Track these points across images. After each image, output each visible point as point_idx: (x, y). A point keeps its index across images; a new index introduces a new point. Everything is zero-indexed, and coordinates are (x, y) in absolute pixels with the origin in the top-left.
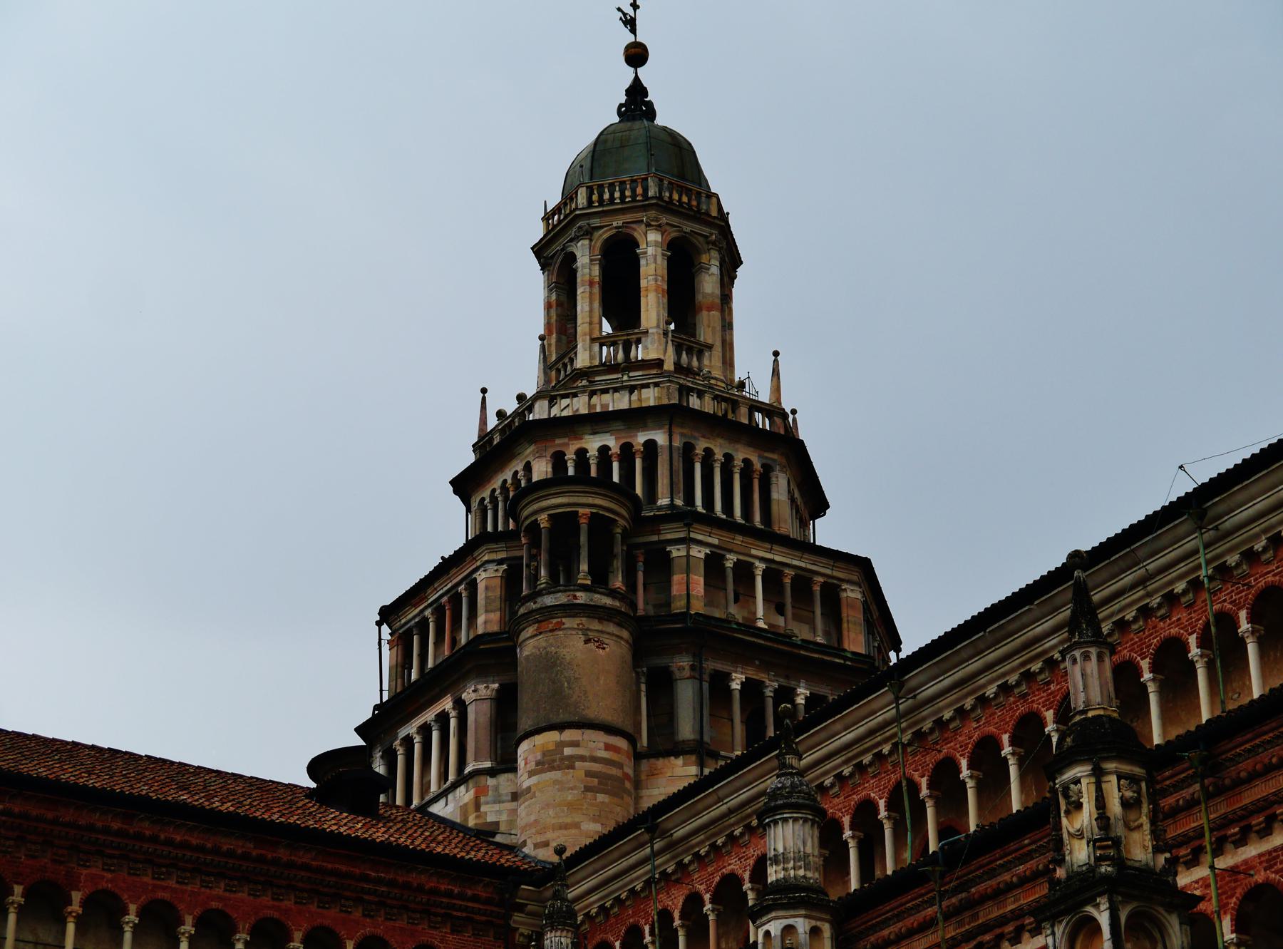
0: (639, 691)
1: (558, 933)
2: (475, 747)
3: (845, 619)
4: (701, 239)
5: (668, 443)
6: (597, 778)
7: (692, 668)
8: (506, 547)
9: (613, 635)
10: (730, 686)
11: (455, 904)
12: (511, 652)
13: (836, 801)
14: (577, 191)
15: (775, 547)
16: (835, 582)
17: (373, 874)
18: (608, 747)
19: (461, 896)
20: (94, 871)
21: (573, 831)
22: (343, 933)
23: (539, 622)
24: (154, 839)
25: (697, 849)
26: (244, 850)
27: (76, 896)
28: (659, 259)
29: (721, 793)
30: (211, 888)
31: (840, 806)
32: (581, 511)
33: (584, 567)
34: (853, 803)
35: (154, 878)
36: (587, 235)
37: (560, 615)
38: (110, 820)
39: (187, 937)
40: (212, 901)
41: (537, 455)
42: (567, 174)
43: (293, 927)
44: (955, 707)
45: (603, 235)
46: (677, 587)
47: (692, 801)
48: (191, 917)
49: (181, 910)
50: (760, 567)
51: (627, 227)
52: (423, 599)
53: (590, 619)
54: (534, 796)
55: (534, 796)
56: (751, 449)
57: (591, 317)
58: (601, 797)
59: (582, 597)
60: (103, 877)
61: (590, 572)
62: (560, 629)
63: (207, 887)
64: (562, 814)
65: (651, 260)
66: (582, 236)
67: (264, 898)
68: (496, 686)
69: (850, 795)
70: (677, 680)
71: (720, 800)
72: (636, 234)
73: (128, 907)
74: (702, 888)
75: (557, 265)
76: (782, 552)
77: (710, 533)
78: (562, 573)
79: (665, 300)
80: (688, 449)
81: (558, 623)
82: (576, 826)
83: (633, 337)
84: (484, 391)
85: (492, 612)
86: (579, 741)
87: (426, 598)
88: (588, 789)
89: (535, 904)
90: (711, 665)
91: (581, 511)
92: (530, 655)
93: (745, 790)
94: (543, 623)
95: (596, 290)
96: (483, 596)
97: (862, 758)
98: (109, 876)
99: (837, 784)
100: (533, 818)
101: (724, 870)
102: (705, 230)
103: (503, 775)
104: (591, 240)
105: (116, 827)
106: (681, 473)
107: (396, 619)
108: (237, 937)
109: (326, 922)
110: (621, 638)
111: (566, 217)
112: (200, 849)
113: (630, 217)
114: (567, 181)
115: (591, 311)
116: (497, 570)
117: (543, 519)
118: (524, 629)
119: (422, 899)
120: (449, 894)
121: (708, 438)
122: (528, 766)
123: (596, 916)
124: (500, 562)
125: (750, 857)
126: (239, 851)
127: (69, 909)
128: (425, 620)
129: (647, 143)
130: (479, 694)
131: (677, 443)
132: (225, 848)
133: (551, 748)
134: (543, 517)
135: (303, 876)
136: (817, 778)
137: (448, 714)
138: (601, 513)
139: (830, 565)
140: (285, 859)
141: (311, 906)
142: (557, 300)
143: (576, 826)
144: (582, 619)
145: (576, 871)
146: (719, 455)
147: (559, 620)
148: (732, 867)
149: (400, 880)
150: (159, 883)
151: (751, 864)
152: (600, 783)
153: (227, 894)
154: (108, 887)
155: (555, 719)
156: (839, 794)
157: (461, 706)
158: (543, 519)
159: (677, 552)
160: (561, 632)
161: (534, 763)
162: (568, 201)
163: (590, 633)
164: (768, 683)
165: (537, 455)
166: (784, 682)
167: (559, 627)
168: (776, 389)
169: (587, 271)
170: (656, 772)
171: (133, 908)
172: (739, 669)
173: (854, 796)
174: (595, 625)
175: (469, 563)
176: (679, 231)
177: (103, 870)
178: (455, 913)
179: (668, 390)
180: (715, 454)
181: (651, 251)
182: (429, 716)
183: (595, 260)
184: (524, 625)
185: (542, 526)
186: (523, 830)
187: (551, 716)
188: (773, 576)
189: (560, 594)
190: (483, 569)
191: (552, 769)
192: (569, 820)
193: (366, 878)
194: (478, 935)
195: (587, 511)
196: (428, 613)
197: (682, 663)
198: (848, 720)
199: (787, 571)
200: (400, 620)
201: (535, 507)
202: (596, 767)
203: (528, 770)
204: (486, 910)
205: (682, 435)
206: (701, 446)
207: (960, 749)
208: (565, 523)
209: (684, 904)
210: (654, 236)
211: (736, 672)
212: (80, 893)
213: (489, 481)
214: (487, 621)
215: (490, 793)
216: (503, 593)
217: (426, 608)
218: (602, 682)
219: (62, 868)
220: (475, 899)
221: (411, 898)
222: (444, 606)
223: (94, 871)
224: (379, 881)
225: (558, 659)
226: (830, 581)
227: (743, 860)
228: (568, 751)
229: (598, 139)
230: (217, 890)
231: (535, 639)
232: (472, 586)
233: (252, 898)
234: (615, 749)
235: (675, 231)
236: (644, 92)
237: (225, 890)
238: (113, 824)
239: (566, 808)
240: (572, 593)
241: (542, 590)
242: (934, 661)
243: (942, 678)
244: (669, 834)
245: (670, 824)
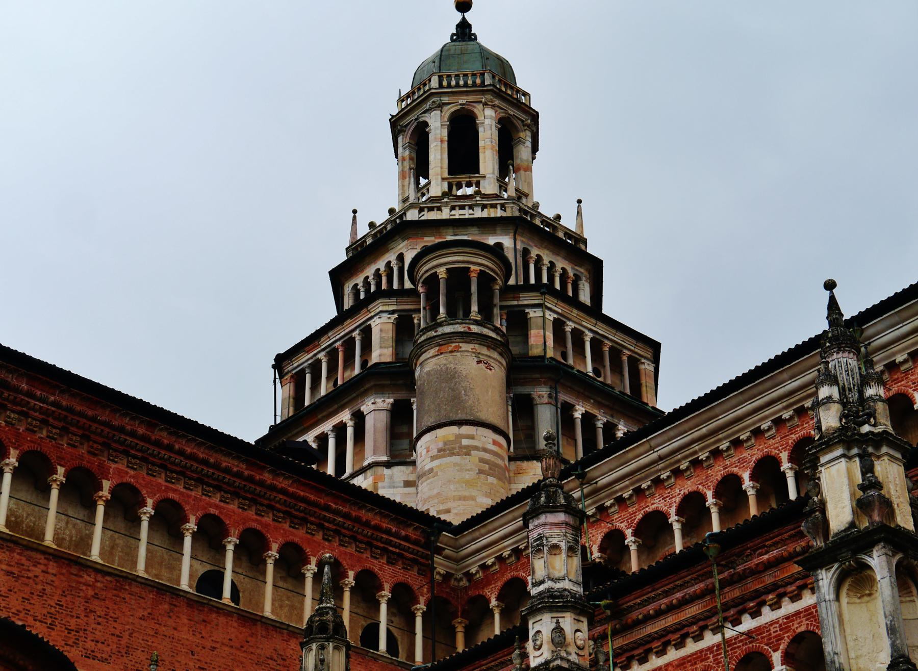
0: (508, 411)
1: (846, 354)
2: (374, 446)
3: (644, 384)
4: (520, 122)
5: (513, 246)
6: (488, 464)
7: (550, 396)
8: (397, 302)
9: (497, 360)
10: (573, 415)
11: (392, 541)
13: (771, 442)
14: (430, 79)
15: (599, 323)
16: (637, 356)
17: (334, 506)
18: (495, 443)
19: (396, 535)
20: (120, 466)
21: (471, 502)
22: (308, 550)
23: (440, 345)
24: (169, 448)
25: (620, 494)
26: (238, 469)
27: (106, 485)
28: (494, 128)
29: (653, 443)
30: (210, 497)
31: (776, 445)
32: (473, 267)
33: (475, 308)
34: (790, 442)
35: (166, 481)
36: (439, 107)
37: (459, 340)
38: (136, 426)
39: (191, 533)
40: (210, 507)
41: (410, 248)
42: (415, 74)
43: (271, 539)
44: (909, 351)
45: (452, 109)
47: (624, 451)
48: (195, 517)
49: (187, 510)
50: (588, 336)
51: (468, 105)
52: (317, 346)
53: (482, 346)
54: (436, 474)
55: (436, 474)
56: (567, 262)
57: (441, 164)
58: (491, 479)
59: (475, 329)
60: (127, 473)
61: (480, 312)
62: (458, 351)
63: (206, 495)
64: (461, 489)
65: (487, 128)
66: (435, 107)
67: (250, 512)
68: (391, 400)
69: (788, 436)
70: (537, 404)
71: (652, 448)
72: (476, 111)
73: (146, 500)
74: (623, 526)
75: (410, 132)
76: (603, 328)
77: (556, 304)
78: (458, 309)
79: (497, 158)
80: (526, 252)
81: (456, 346)
82: (473, 498)
83: (474, 179)
84: (355, 212)
85: (385, 348)
86: (474, 435)
87: (319, 345)
88: (481, 472)
89: (451, 549)
90: (563, 397)
91: (473, 267)
92: (431, 371)
93: (679, 438)
94: (443, 347)
95: (445, 145)
96: (378, 336)
97: (804, 403)
98: (132, 472)
99: (774, 427)
100: (435, 491)
101: (647, 509)
102: (522, 116)
103: (396, 467)
104: (441, 112)
105: (141, 432)
106: (522, 268)
107: (290, 363)
108: (229, 540)
109: (296, 540)
110: (502, 365)
111: (425, 92)
112: (205, 462)
113: (471, 98)
114: (416, 77)
115: (442, 159)
116: (389, 318)
117: (442, 273)
118: (425, 351)
119: (368, 532)
120: (388, 532)
121: (539, 248)
122: (429, 453)
123: (508, 558)
124: (393, 312)
125: (675, 496)
126: (235, 469)
127: (101, 493)
128: (319, 362)
129: (481, 53)
131: (520, 246)
132: (224, 464)
133: (451, 439)
134: (441, 270)
135: (281, 499)
136: (754, 423)
137: (345, 424)
138: (487, 271)
139: (634, 344)
140: (269, 482)
141: (285, 525)
142: (410, 155)
143: (473, 498)
144: (476, 345)
145: (494, 520)
146: (546, 260)
147: (457, 344)
148: (656, 505)
149: (354, 514)
150: (170, 485)
151: (677, 501)
152: (490, 469)
153: (222, 504)
154: (131, 482)
155: (454, 417)
156: (775, 436)
157: (359, 418)
158: (442, 273)
159: (533, 313)
160: (459, 354)
161: (436, 450)
162: (421, 86)
163: (481, 357)
164: (599, 417)
165: (410, 248)
166: (610, 419)
167: (457, 349)
168: (580, 225)
169: (439, 132)
170: (521, 472)
171: (150, 502)
172: (581, 403)
173: (793, 436)
174: (484, 351)
175: (363, 314)
176: (506, 113)
177: (128, 467)
178: (391, 548)
179: (512, 209)
180: (543, 260)
181: (487, 122)
182: (327, 427)
183: (445, 125)
184: (426, 348)
185: (440, 277)
186: (426, 501)
187: (451, 415)
188: (597, 344)
189: (458, 325)
190: (378, 316)
191: (453, 454)
192: (466, 494)
193: (327, 508)
194: (407, 569)
195: (477, 268)
196: (321, 356)
197: (541, 393)
198: (796, 370)
199: (606, 342)
200: (293, 365)
201: (435, 263)
202: (487, 456)
203: (430, 456)
204: (414, 549)
205: (522, 242)
206: (534, 252)
207: (912, 386)
208: (458, 276)
209: (603, 540)
210: (489, 112)
211: (579, 405)
212: (109, 482)
213: (362, 271)
214: (381, 353)
215: (386, 480)
216: (394, 335)
217: (319, 352)
218: (490, 393)
219: (95, 459)
221: (360, 530)
222: (338, 349)
223: (120, 466)
224: (337, 512)
225: (456, 373)
226: (634, 355)
227: (668, 499)
228: (465, 442)
229: (443, 48)
230: (214, 499)
231: (436, 358)
232: (367, 332)
233: (240, 510)
234: (500, 446)
235: (503, 113)
236: (470, 26)
237: (221, 501)
238: (139, 430)
239: (464, 485)
240: (467, 325)
241: (442, 322)
242: (896, 311)
243: (901, 325)
244: (594, 481)
245: (596, 473)
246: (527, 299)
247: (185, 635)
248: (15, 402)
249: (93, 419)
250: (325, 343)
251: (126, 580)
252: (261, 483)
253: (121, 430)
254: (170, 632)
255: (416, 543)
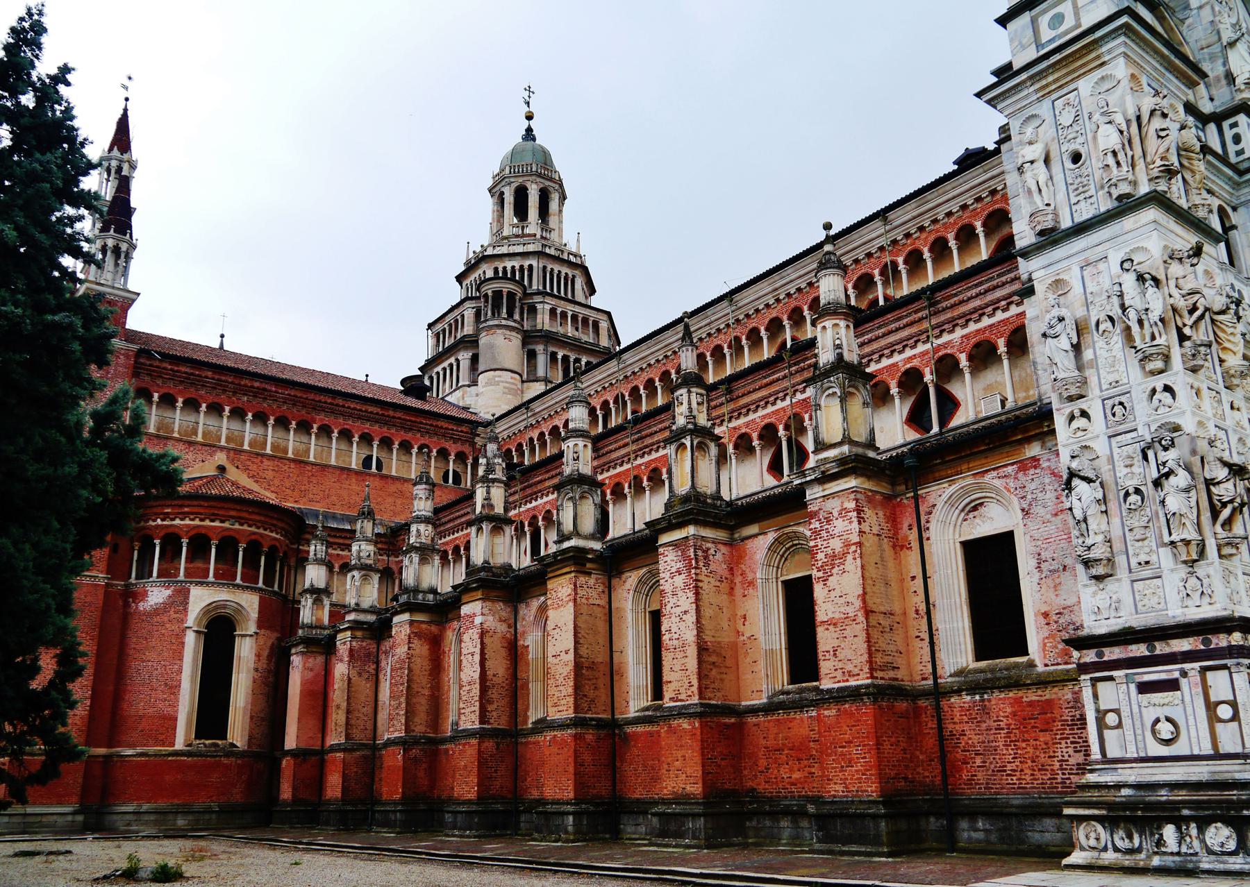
12: (477, 341)
19: (457, 431)
27: (315, 426)
33: (505, 311)
46: (539, 320)
50: (570, 314)
59: (504, 322)
74: (545, 430)
80: (545, 268)
90: (551, 349)
102: (554, 185)
112: (361, 410)
113: (525, 178)
120: (452, 430)
130: (464, 356)
146: (556, 272)
159: (539, 306)
168: (578, 247)
174: (508, 332)
182: (446, 364)
188: (574, 317)
193: (422, 423)
197: (539, 348)
202: (507, 385)
208: (498, 294)
210: (534, 186)
214: (468, 329)
220: (462, 431)
224: (426, 424)
232: (463, 316)
234: (515, 379)
236: (532, 130)
246: (537, 299)
247: (354, 487)
248: (270, 396)
249: (307, 399)
250: (447, 319)
251: (325, 467)
252: (388, 416)
253: (320, 401)
254: (348, 487)
255: (467, 433)
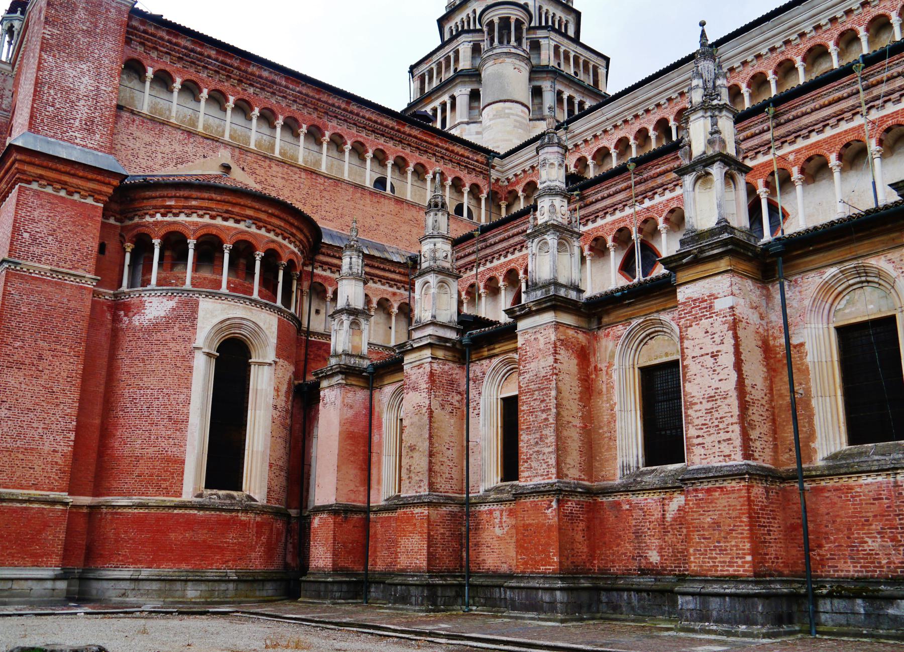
7: (551, 87)
12: (480, 75)
18: (522, 111)
24: (358, 115)
33: (513, 39)
46: (543, 57)
50: (572, 55)
58: (520, 131)
59: (513, 50)
61: (516, 41)
68: (470, 90)
74: (586, 155)
88: (515, 127)
90: (559, 87)
98: (339, 127)
109: (422, 162)
112: (375, 122)
120: (468, 158)
124: (470, 42)
128: (432, 69)
130: (462, 92)
157: (453, 98)
158: (496, 20)
159: (543, 42)
174: (517, 62)
182: (436, 103)
188: (576, 59)
191: (501, 117)
193: (437, 146)
197: (546, 85)
202: (518, 118)
208: (505, 22)
214: (465, 64)
220: (477, 161)
224: (442, 148)
228: (507, 111)
232: (457, 53)
246: (541, 33)
247: (369, 208)
248: (280, 91)
249: (319, 100)
250: (435, 58)
251: (338, 181)
252: (404, 133)
253: (333, 105)
254: (362, 207)
255: (482, 163)
